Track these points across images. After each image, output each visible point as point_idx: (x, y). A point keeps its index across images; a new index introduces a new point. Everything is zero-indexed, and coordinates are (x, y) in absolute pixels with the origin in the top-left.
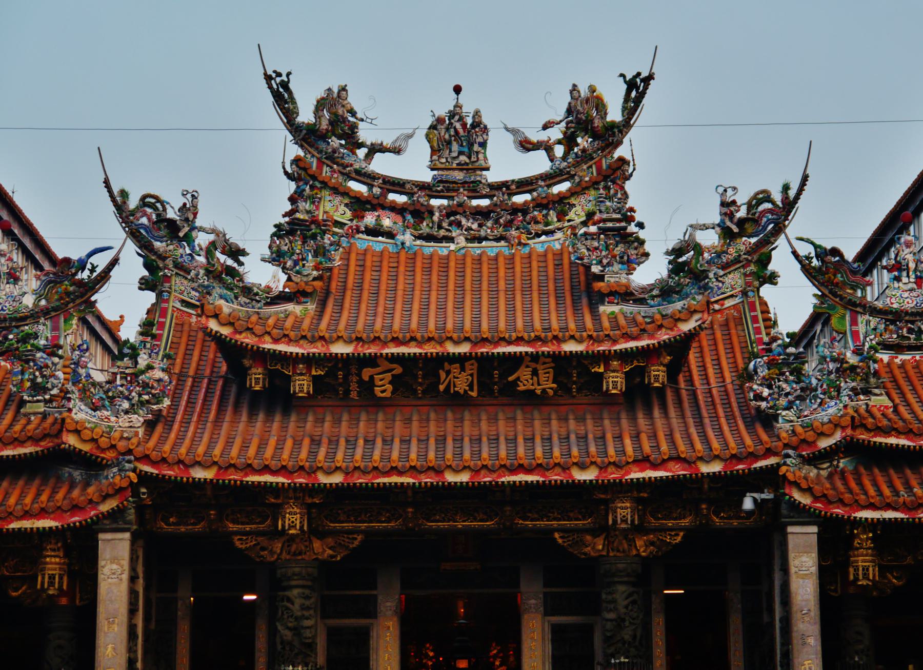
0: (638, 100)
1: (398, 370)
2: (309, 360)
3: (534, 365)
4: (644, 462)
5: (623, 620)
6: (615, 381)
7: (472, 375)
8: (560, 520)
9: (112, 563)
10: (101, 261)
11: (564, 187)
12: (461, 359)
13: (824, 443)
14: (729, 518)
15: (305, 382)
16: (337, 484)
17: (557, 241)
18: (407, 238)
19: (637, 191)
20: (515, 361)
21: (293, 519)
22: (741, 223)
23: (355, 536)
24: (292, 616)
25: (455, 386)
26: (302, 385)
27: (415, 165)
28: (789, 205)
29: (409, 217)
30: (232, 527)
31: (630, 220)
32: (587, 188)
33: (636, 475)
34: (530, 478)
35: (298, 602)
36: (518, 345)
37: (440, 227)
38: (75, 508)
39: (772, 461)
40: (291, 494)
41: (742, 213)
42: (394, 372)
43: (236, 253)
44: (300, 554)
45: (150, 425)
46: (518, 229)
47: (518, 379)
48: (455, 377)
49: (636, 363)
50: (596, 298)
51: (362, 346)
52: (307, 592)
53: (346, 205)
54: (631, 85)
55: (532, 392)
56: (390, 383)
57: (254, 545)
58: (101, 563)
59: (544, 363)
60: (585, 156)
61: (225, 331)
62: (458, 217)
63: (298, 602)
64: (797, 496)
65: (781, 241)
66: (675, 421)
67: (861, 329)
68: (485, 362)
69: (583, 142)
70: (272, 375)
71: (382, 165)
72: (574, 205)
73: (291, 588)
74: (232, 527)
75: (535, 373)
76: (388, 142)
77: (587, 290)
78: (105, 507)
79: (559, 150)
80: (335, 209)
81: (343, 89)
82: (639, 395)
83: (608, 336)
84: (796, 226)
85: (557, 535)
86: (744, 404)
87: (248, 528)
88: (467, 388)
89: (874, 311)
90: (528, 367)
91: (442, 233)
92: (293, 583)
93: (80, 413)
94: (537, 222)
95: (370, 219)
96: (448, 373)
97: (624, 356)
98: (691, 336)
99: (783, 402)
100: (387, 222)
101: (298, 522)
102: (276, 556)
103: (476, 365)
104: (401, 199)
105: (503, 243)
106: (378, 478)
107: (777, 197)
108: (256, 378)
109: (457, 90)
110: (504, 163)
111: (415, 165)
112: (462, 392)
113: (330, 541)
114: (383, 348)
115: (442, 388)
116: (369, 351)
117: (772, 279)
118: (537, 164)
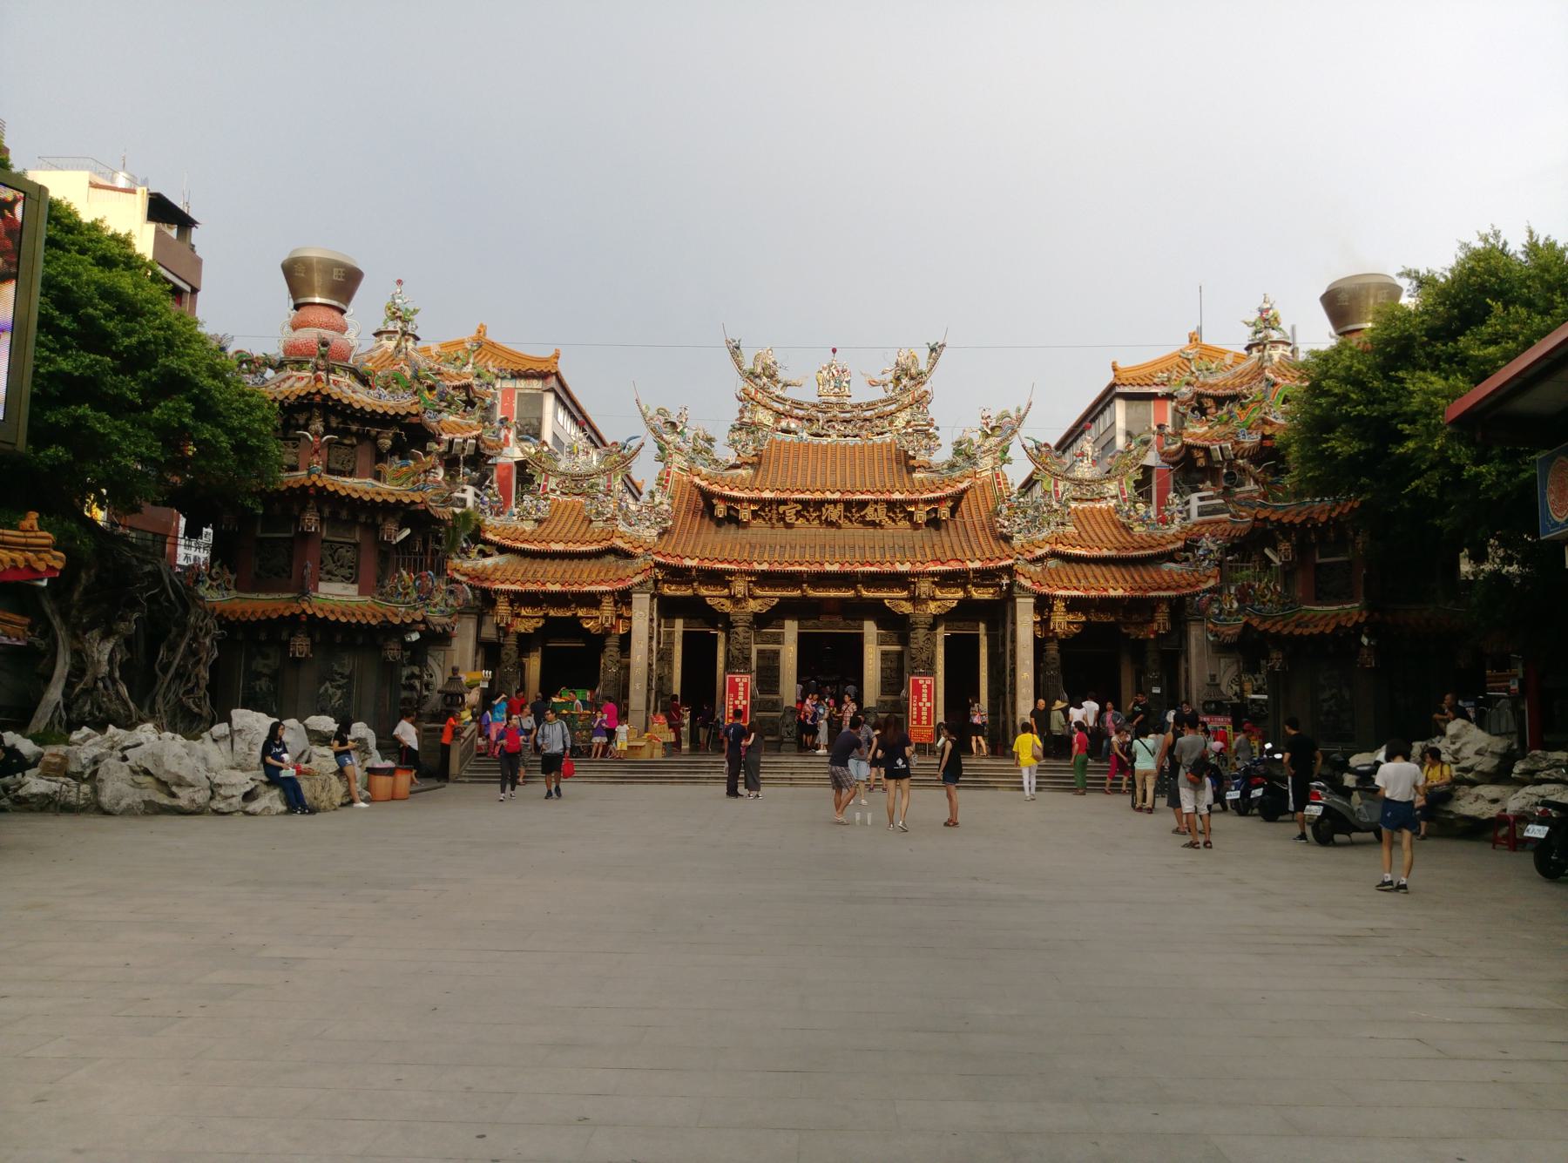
0: (936, 360)
2: (751, 501)
4: (937, 561)
10: (634, 444)
11: (893, 407)
12: (835, 502)
13: (1039, 552)
17: (888, 438)
18: (805, 435)
19: (934, 410)
20: (863, 504)
21: (739, 587)
22: (993, 429)
26: (745, 515)
27: (808, 394)
28: (1020, 420)
31: (930, 425)
33: (932, 568)
34: (872, 569)
38: (621, 580)
39: (1010, 562)
41: (993, 424)
43: (710, 440)
45: (660, 535)
50: (912, 470)
54: (933, 350)
60: (905, 390)
61: (704, 484)
63: (742, 634)
64: (1023, 581)
65: (1015, 439)
66: (955, 539)
67: (1061, 488)
68: (848, 505)
69: (905, 381)
70: (729, 508)
71: (789, 393)
77: (906, 463)
79: (891, 386)
80: (765, 417)
82: (934, 523)
84: (1023, 431)
86: (993, 530)
89: (1068, 479)
93: (622, 527)
95: (783, 424)
97: (927, 502)
98: (965, 491)
99: (1016, 528)
100: (793, 426)
104: (801, 413)
107: (1013, 415)
108: (721, 510)
109: (834, 351)
110: (860, 393)
117: (1009, 461)
118: (878, 394)
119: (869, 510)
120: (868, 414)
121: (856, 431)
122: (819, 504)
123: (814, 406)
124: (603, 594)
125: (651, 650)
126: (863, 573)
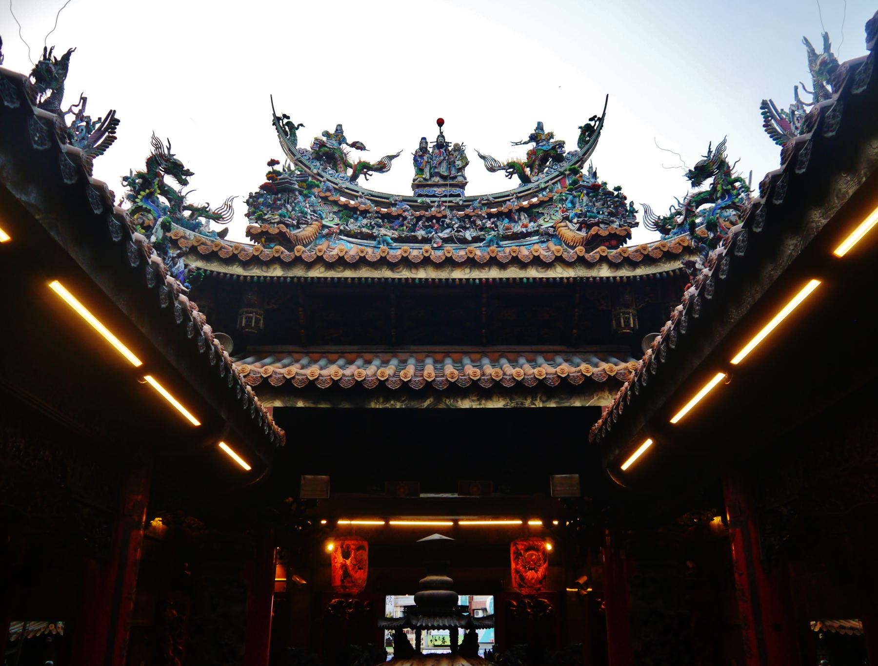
27: (398, 182)
43: (179, 171)
53: (334, 213)
72: (543, 214)
76: (373, 160)
81: (339, 127)
111: (398, 182)
123: (405, 200)
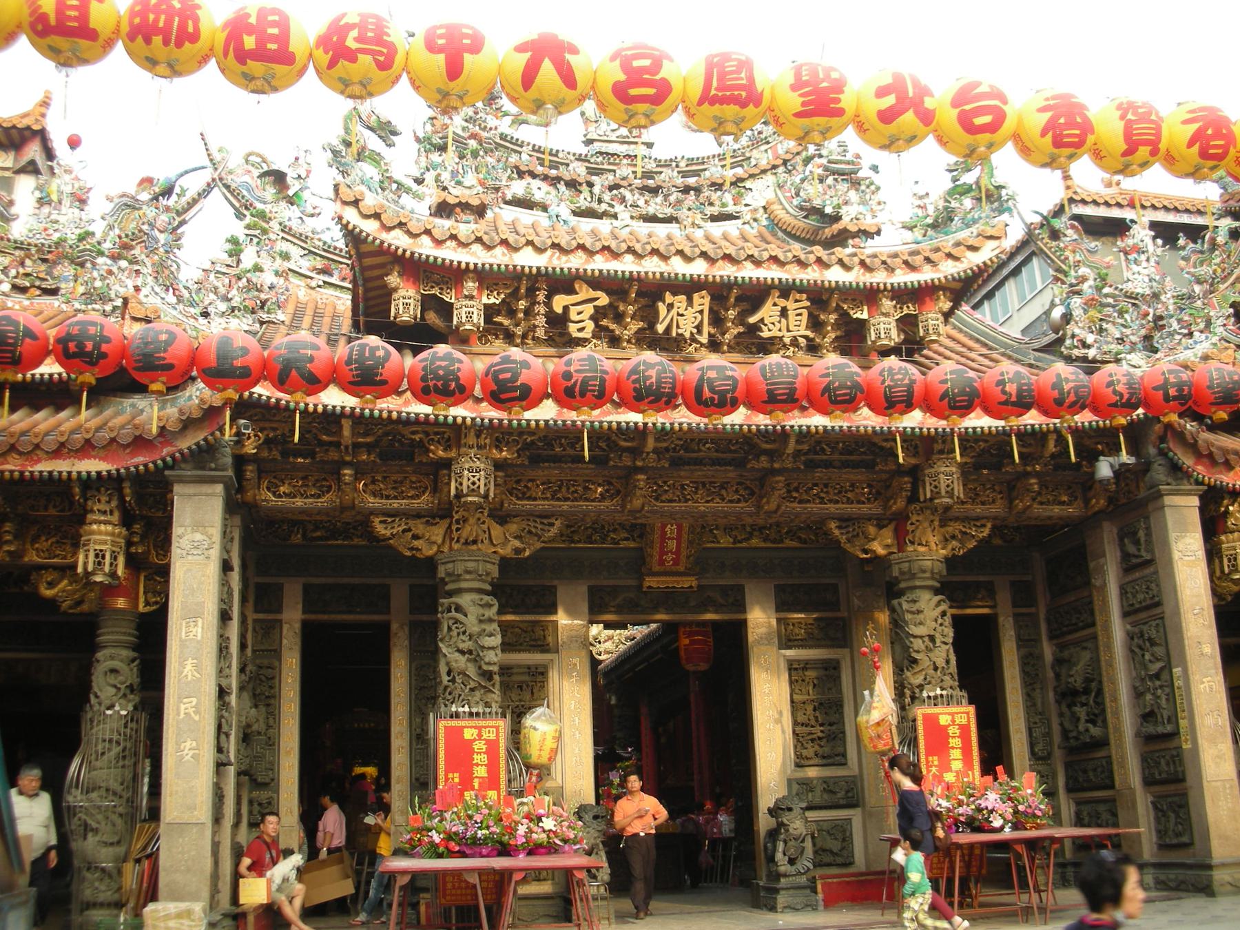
1: (604, 300)
3: (782, 303)
5: (932, 638)
6: (884, 326)
7: (701, 312)
8: (837, 502)
9: (193, 531)
10: (193, 184)
12: (689, 287)
14: (1048, 503)
15: (474, 310)
16: (546, 422)
18: (565, 212)
23: (552, 520)
24: (464, 633)
25: (678, 327)
29: (562, 187)
30: (372, 502)
32: (764, 172)
35: (473, 613)
36: (769, 269)
37: (600, 201)
40: (472, 440)
42: (596, 303)
44: (475, 542)
46: (689, 209)
47: (762, 320)
48: (679, 315)
49: (906, 311)
51: (559, 258)
52: (487, 598)
55: (781, 338)
56: (592, 318)
57: (404, 531)
58: (177, 530)
59: (797, 301)
62: (622, 190)
70: (428, 302)
73: (459, 591)
74: (372, 502)
75: (784, 312)
78: (186, 443)
83: (884, 262)
85: (833, 525)
87: (396, 504)
88: (695, 331)
90: (775, 305)
91: (604, 207)
92: (464, 585)
94: (711, 204)
96: (670, 307)
101: (482, 483)
102: (435, 548)
103: (707, 300)
105: (674, 225)
106: (609, 414)
112: (687, 335)
113: (513, 527)
114: (587, 262)
115: (660, 328)
116: (569, 265)
119: (768, 312)
120: (692, 181)
121: (669, 211)
122: (651, 292)
124: (92, 484)
125: (223, 650)
126: (805, 435)
